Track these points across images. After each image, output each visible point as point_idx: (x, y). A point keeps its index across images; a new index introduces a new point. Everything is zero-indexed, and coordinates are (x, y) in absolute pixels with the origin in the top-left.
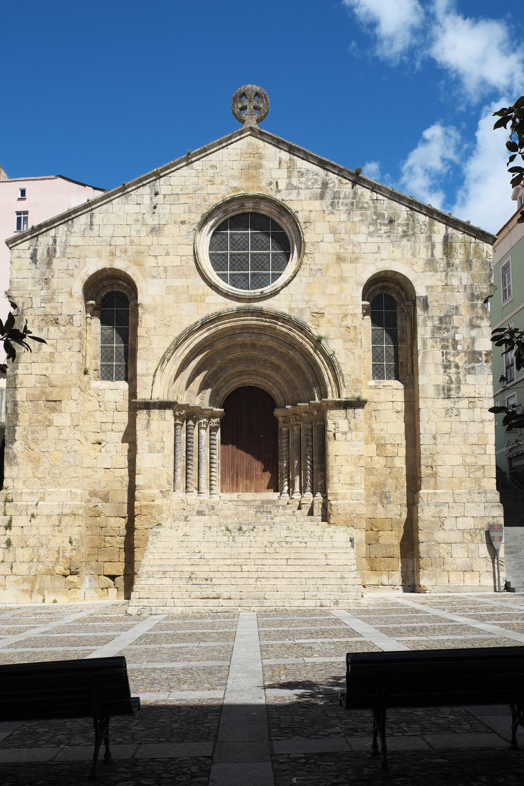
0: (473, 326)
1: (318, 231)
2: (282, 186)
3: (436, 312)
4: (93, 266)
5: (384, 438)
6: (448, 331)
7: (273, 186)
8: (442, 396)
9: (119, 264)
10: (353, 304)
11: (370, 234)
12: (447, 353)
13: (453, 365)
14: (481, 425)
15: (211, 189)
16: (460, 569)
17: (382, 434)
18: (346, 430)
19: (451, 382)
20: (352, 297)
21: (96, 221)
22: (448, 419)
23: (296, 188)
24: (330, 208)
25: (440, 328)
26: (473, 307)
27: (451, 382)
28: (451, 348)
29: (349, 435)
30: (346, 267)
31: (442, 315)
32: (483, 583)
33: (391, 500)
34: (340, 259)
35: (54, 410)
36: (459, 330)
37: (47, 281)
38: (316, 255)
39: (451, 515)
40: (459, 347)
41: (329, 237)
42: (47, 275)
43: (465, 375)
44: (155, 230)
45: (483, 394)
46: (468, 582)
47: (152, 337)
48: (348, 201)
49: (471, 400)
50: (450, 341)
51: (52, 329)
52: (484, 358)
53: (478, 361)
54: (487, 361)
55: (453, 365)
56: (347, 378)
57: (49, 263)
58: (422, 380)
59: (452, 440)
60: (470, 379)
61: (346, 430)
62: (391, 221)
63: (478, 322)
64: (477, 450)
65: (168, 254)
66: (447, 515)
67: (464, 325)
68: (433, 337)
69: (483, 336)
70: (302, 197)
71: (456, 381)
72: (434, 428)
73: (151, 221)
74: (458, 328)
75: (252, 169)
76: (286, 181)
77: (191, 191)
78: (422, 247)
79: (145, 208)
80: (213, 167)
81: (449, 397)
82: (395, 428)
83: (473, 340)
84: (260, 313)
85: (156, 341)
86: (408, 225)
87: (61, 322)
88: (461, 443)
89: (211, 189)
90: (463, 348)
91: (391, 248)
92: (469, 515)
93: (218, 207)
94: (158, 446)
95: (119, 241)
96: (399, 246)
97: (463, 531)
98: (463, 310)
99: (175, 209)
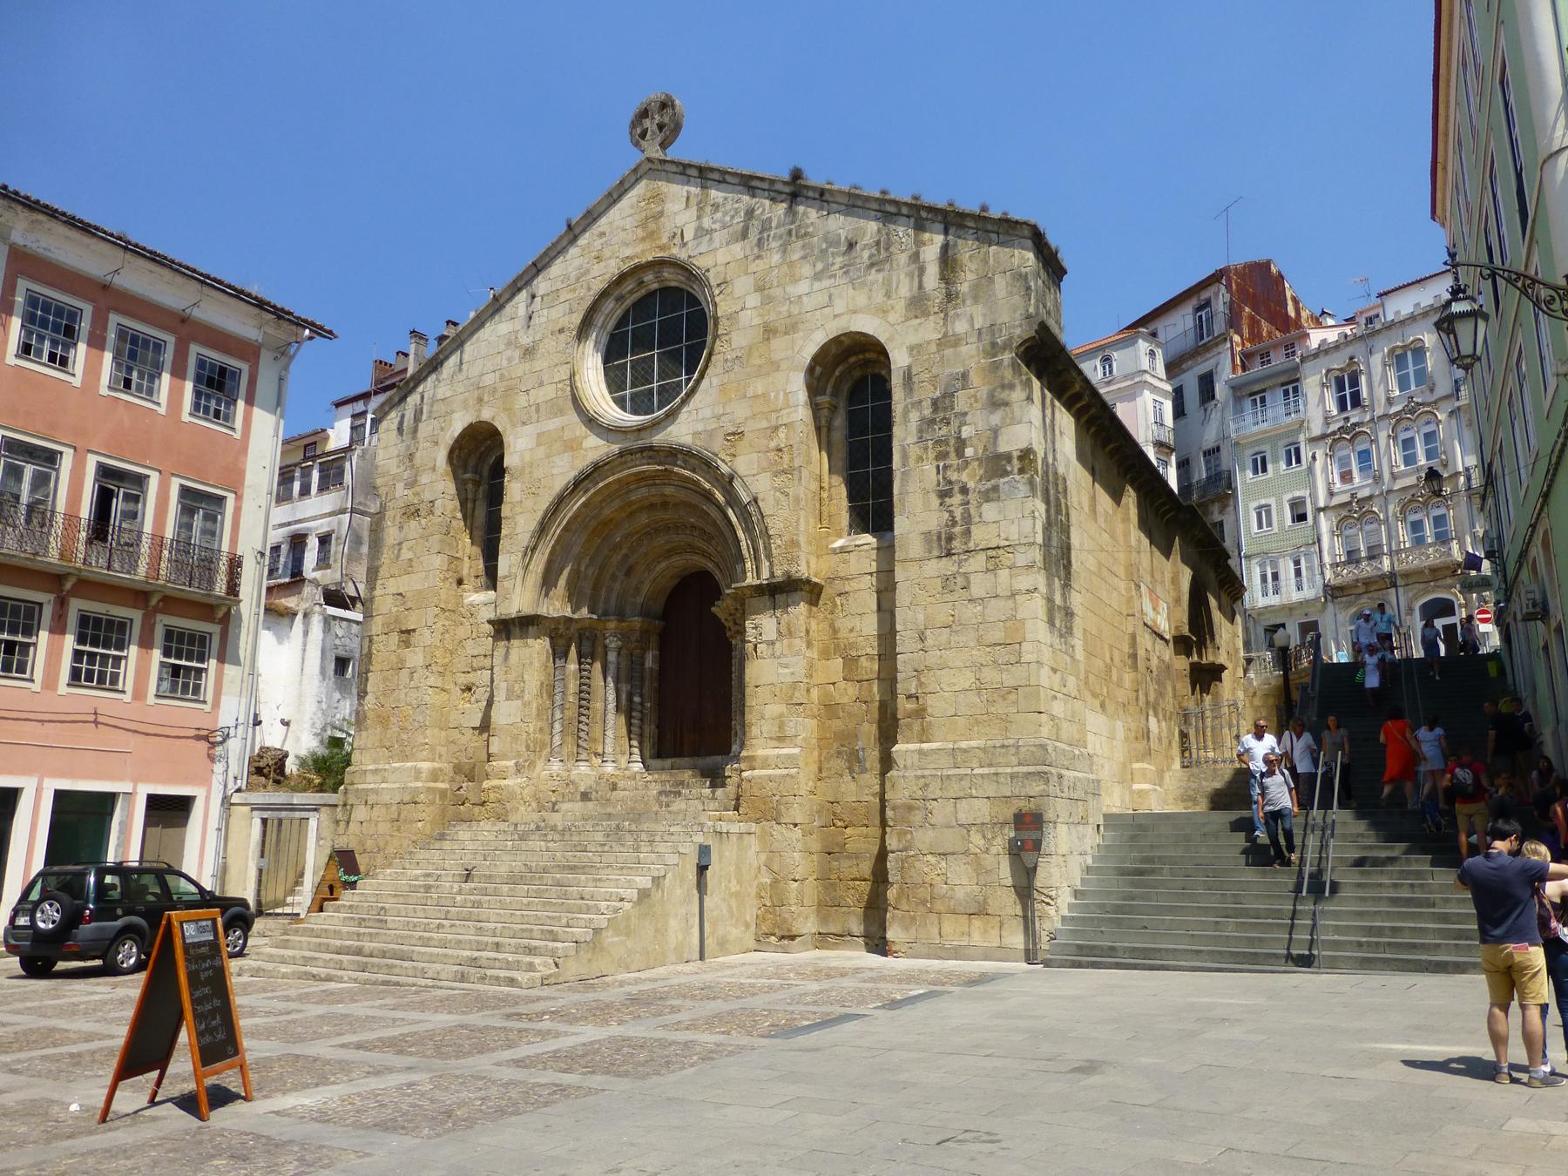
0: (995, 404)
1: (737, 293)
2: (688, 236)
3: (927, 393)
4: (458, 426)
5: (852, 645)
6: (948, 423)
7: (677, 240)
8: (936, 553)
9: (486, 415)
10: (789, 406)
11: (817, 277)
12: (946, 467)
13: (956, 488)
14: (1010, 603)
15: (597, 270)
16: (962, 910)
17: (852, 637)
18: (774, 636)
19: (954, 523)
20: (786, 394)
21: (466, 357)
22: (948, 597)
23: (710, 232)
24: (756, 250)
25: (932, 421)
26: (996, 367)
27: (954, 523)
28: (953, 455)
29: (778, 645)
30: (779, 345)
31: (938, 394)
32: (1007, 941)
33: (868, 765)
34: (769, 332)
35: (407, 644)
36: (968, 418)
37: (411, 456)
38: (733, 335)
39: (946, 794)
40: (969, 452)
41: (753, 300)
42: (413, 449)
43: (980, 505)
44: (529, 352)
45: (1014, 537)
46: (977, 939)
47: (518, 518)
48: (782, 230)
49: (990, 553)
50: (952, 442)
51: (413, 523)
52: (1016, 464)
53: (1007, 473)
54: (1021, 471)
55: (956, 488)
56: (776, 542)
57: (415, 430)
58: (901, 524)
59: (955, 638)
60: (990, 511)
61: (774, 636)
62: (851, 245)
63: (1004, 395)
64: (1003, 655)
65: (541, 384)
66: (938, 794)
67: (979, 406)
68: (921, 439)
69: (1016, 421)
70: (716, 244)
71: (963, 519)
72: (921, 617)
73: (525, 340)
74: (966, 414)
75: (651, 220)
76: (693, 225)
77: (573, 280)
78: (902, 276)
79: (518, 324)
80: (603, 234)
81: (949, 554)
82: (864, 626)
83: (995, 432)
84: (650, 452)
85: (521, 520)
86: (878, 243)
87: (422, 513)
88: (972, 644)
89: (597, 270)
90: (976, 452)
91: (851, 291)
92: (981, 793)
93: (604, 295)
94: (517, 687)
95: (489, 380)
96: (863, 284)
97: (967, 827)
98: (975, 379)
99: (556, 313)
